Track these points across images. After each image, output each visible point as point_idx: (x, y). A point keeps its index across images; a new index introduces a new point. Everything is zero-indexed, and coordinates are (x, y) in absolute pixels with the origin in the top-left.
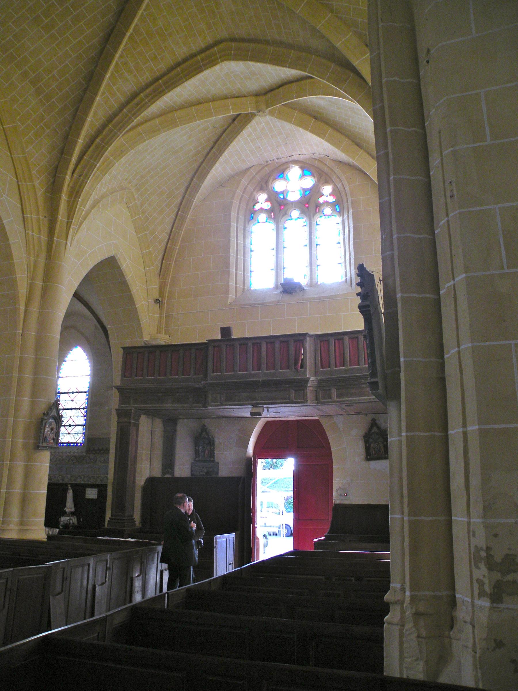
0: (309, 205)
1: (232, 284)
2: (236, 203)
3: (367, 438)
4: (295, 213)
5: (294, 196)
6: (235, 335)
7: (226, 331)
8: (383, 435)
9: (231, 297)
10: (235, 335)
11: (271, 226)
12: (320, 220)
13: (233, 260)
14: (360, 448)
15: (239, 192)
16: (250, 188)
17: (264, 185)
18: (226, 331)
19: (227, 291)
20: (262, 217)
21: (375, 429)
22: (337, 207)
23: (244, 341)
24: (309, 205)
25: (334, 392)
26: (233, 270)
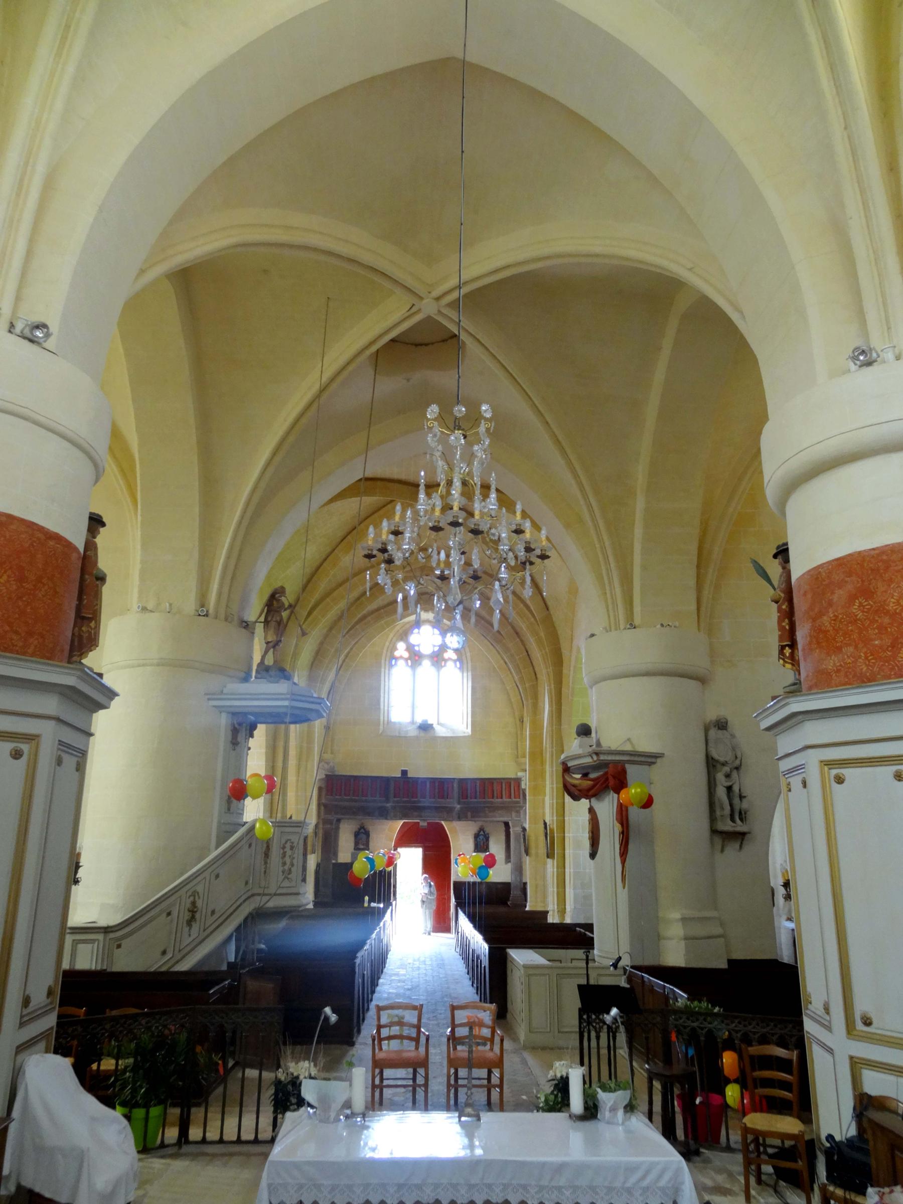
0: (437, 658)
1: (382, 718)
2: (385, 651)
3: (476, 836)
4: (426, 663)
6: (409, 775)
7: (404, 773)
9: (381, 727)
10: (409, 775)
11: (409, 671)
13: (382, 699)
14: (471, 845)
15: (387, 644)
16: (395, 639)
17: (404, 636)
18: (404, 773)
19: (379, 724)
20: (401, 663)
21: (482, 833)
22: (458, 663)
23: (416, 781)
24: (437, 658)
25: (469, 814)
26: (382, 707)
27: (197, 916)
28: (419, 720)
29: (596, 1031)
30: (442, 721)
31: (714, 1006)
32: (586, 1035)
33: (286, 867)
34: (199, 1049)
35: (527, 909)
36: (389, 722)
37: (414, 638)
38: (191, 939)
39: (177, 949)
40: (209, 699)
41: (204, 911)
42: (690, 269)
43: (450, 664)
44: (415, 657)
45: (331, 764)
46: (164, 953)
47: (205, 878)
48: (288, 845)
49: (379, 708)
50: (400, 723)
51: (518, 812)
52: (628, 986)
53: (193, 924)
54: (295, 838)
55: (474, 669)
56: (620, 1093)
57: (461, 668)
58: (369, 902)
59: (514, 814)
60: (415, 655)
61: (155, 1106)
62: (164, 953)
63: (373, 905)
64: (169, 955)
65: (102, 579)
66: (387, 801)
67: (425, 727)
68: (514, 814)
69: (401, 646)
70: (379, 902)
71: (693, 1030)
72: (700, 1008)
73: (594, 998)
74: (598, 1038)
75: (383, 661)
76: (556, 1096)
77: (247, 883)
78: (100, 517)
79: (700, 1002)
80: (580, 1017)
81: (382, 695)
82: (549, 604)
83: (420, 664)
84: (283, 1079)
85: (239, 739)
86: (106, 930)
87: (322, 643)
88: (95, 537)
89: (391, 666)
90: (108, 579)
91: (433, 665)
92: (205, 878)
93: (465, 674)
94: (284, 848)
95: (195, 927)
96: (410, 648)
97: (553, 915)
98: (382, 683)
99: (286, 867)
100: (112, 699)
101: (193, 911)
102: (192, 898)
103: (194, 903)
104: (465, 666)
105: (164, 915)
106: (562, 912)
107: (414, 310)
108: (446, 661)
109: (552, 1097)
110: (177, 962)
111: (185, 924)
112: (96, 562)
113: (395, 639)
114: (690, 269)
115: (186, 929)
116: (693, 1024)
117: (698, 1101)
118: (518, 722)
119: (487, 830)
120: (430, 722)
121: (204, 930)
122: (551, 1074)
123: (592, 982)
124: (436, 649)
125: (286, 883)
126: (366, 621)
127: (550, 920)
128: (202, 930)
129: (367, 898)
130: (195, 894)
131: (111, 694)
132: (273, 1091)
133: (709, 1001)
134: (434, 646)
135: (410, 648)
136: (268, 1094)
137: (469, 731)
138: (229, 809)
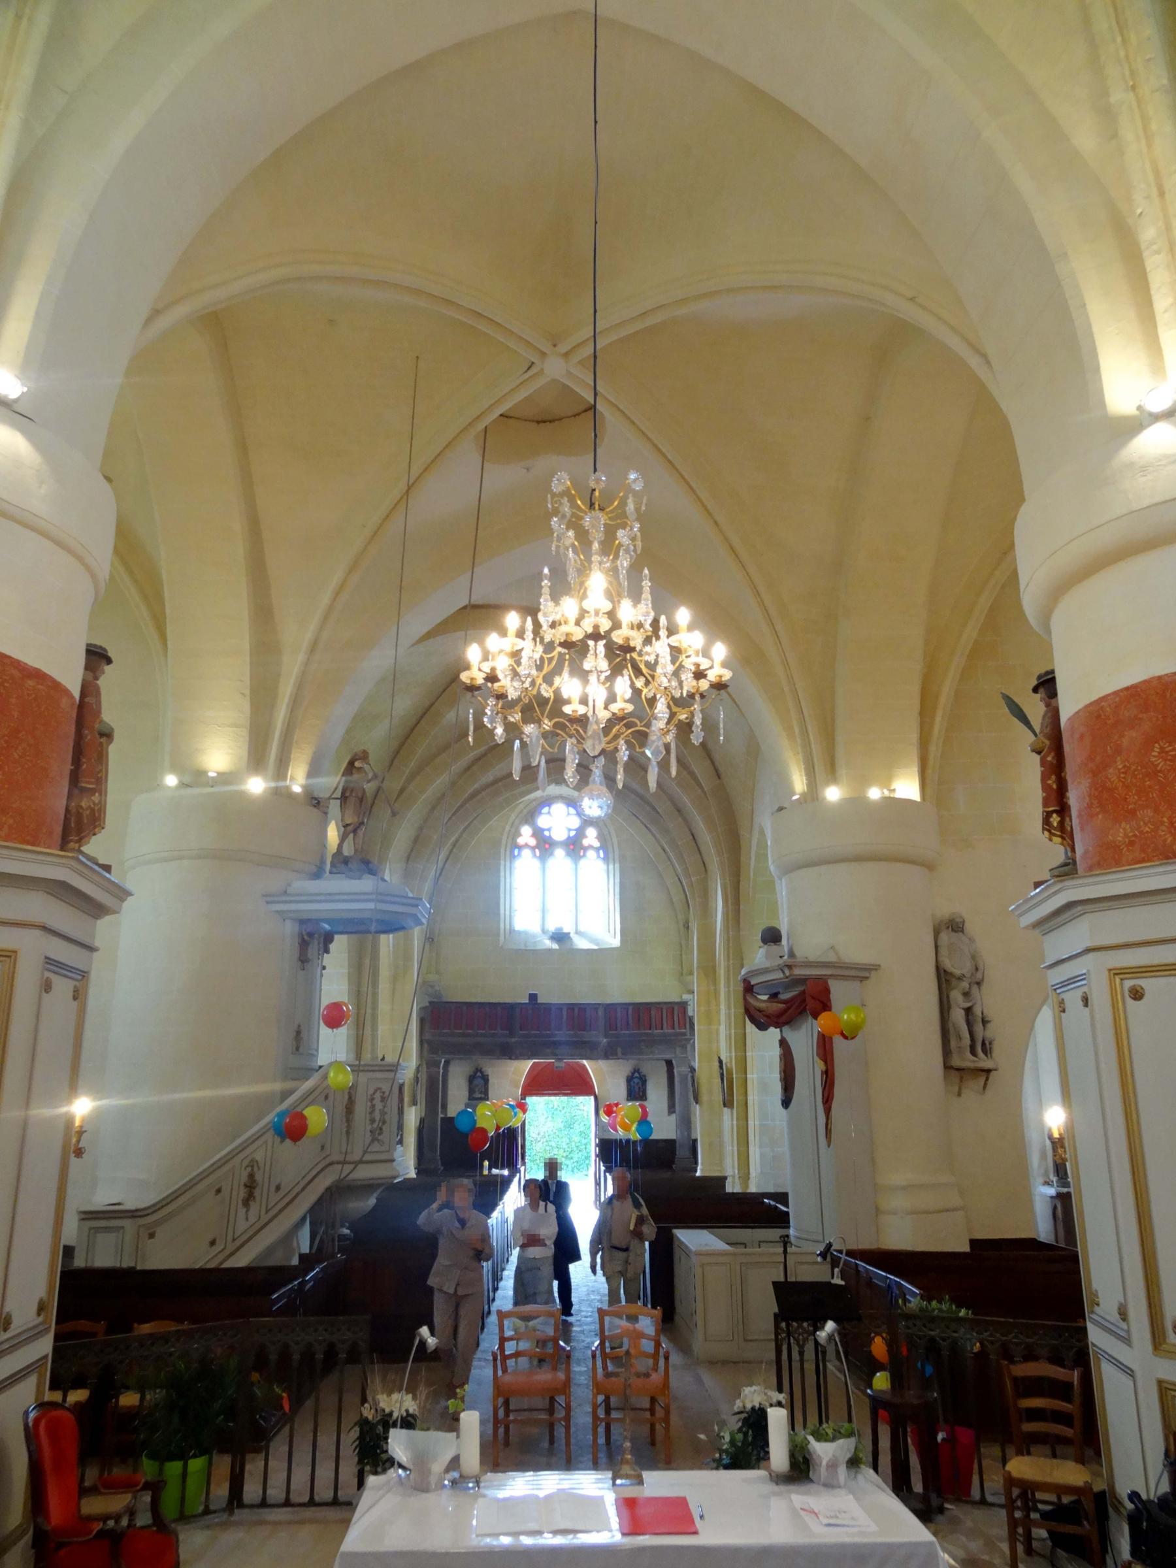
0: (574, 846)
2: (504, 838)
3: (629, 1080)
4: (560, 853)
5: (559, 835)
7: (533, 997)
8: (643, 1081)
9: (502, 938)
11: (536, 863)
12: (583, 862)
13: (502, 901)
15: (508, 828)
16: (517, 821)
17: (530, 817)
18: (533, 997)
19: (498, 935)
20: (526, 853)
22: (601, 852)
23: (548, 1007)
24: (574, 846)
25: (619, 1050)
26: (502, 912)
27: (257, 1193)
28: (551, 927)
29: (798, 1344)
30: (581, 928)
31: (959, 1306)
32: (785, 1348)
33: (375, 1126)
34: (255, 1376)
35: (698, 1174)
36: (512, 931)
37: (543, 821)
38: (249, 1223)
39: (230, 1238)
40: (268, 903)
41: (266, 1185)
42: (912, 299)
43: (591, 854)
44: (545, 845)
45: (437, 988)
46: (213, 1243)
47: (266, 1142)
48: (378, 1095)
49: (499, 914)
50: (526, 933)
51: (684, 1047)
52: (843, 1283)
53: (251, 1203)
54: (386, 1087)
55: (622, 859)
56: (841, 1441)
57: (606, 859)
58: (490, 1169)
59: (678, 1050)
60: (545, 842)
61: (195, 1456)
62: (213, 1243)
63: (495, 1171)
64: (219, 1247)
65: (108, 735)
66: (512, 1034)
67: (560, 937)
68: (678, 1050)
69: (526, 832)
70: (503, 1168)
71: (932, 1340)
72: (940, 1310)
73: (798, 1303)
74: (801, 1353)
75: (502, 851)
76: (745, 1435)
77: (323, 1147)
78: (105, 650)
79: (940, 1302)
80: (777, 1326)
81: (502, 895)
82: (721, 769)
83: (551, 854)
84: (370, 1417)
85: (309, 956)
86: (133, 1214)
87: (421, 829)
88: (96, 678)
89: (513, 857)
90: (117, 735)
91: (568, 854)
92: (266, 1142)
93: (611, 867)
94: (372, 1100)
95: (254, 1207)
96: (538, 833)
97: (733, 1183)
98: (502, 879)
99: (375, 1126)
100: (122, 900)
101: (251, 1186)
102: (249, 1169)
103: (251, 1176)
104: (611, 855)
105: (213, 1191)
106: (745, 1177)
107: (534, 370)
108: (585, 849)
109: (740, 1436)
110: (232, 1254)
111: (240, 1202)
112: (98, 712)
113: (517, 821)
114: (912, 299)
115: (242, 1211)
116: (932, 1333)
117: (940, 1437)
118: (682, 928)
119: (644, 1071)
120: (565, 931)
121: (267, 1212)
122: (738, 1404)
123: (791, 1279)
124: (573, 834)
125: (375, 1147)
126: (478, 797)
127: (729, 1188)
128: (263, 1211)
129: (486, 1163)
130: (253, 1164)
131: (122, 894)
132: (358, 1434)
133: (953, 1300)
134: (570, 830)
135: (538, 833)
136: (351, 1437)
137: (616, 942)
138: (297, 1049)
